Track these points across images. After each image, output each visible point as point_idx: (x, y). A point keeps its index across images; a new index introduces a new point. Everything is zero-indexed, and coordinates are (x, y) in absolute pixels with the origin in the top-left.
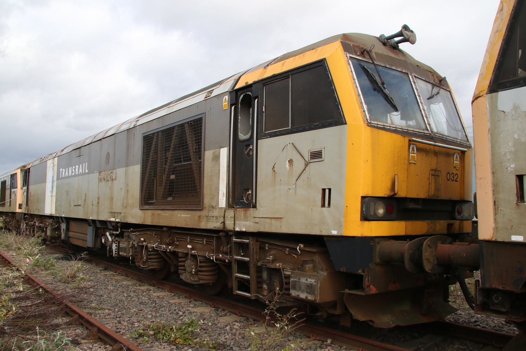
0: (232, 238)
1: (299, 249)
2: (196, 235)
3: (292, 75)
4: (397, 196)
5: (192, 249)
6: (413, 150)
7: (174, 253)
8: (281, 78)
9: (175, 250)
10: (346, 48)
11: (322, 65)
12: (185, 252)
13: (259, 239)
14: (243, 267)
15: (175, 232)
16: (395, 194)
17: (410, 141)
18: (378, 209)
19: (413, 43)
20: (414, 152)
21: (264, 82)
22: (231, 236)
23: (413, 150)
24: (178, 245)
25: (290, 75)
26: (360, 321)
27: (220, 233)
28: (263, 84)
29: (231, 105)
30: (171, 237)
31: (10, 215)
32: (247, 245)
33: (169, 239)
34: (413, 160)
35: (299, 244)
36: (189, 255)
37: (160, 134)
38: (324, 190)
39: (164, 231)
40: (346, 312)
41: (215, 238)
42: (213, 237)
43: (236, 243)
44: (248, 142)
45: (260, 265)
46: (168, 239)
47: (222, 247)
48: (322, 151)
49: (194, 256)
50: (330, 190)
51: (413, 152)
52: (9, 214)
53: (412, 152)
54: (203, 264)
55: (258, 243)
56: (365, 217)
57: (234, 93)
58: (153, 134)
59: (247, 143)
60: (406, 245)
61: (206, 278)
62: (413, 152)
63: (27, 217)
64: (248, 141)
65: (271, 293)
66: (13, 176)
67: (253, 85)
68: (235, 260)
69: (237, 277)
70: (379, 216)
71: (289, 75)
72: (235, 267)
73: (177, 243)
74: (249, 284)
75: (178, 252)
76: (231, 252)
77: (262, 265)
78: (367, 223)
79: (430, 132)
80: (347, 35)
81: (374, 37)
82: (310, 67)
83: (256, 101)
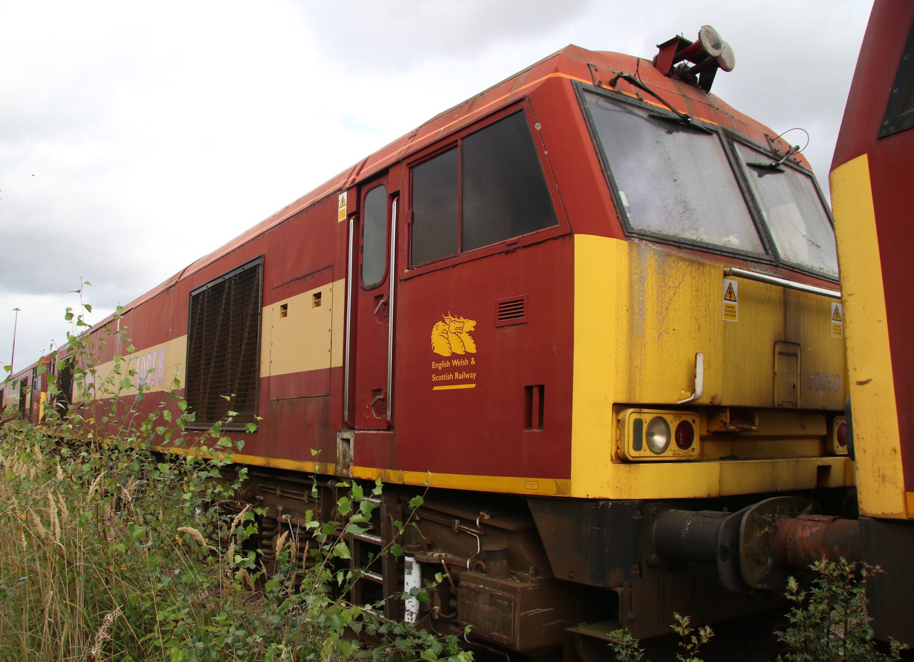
6: (730, 293)
15: (258, 477)
20: (732, 296)
24: (262, 501)
25: (460, 142)
28: (408, 165)
30: (250, 485)
33: (246, 489)
34: (731, 315)
35: (481, 510)
46: (244, 490)
51: (731, 297)
58: (221, 285)
60: (718, 521)
62: (731, 297)
67: (391, 171)
68: (355, 539)
71: (457, 141)
73: (262, 498)
81: (644, 59)
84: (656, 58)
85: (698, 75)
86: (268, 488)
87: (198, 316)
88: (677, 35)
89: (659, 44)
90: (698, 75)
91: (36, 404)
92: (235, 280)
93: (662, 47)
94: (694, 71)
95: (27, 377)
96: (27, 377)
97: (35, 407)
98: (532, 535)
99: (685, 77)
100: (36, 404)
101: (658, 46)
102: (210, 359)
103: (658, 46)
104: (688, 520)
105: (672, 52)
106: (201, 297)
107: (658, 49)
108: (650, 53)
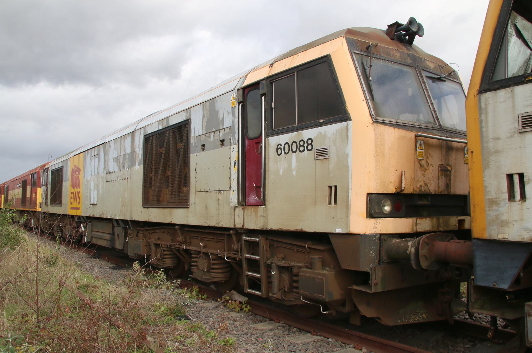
0: (242, 236)
1: (307, 247)
2: (208, 233)
3: (297, 71)
4: (403, 192)
5: (204, 247)
7: (187, 251)
8: (287, 75)
9: (188, 248)
10: (351, 44)
11: (326, 61)
12: (199, 250)
13: (268, 237)
14: (254, 265)
16: (402, 191)
17: (416, 136)
18: (384, 206)
19: (421, 36)
21: (270, 79)
22: (242, 234)
23: (421, 146)
26: (367, 318)
27: (230, 230)
28: (270, 81)
29: (239, 103)
31: (31, 214)
32: (256, 244)
36: (201, 253)
37: (171, 131)
38: (330, 187)
39: (176, 229)
40: (356, 310)
41: (226, 236)
42: (224, 234)
43: (246, 241)
44: (257, 140)
45: (270, 263)
47: (233, 245)
48: (327, 148)
49: (207, 254)
50: (336, 187)
51: (421, 148)
52: (29, 213)
53: (420, 148)
54: (214, 262)
55: (268, 242)
56: (371, 215)
57: (241, 91)
59: (256, 141)
61: (218, 276)
63: (46, 216)
64: (257, 138)
65: (281, 292)
66: (33, 175)
69: (247, 276)
70: (385, 212)
71: (295, 72)
72: (245, 265)
74: (260, 282)
75: (191, 250)
76: (241, 250)
77: (272, 263)
78: (372, 220)
79: (439, 127)
80: (353, 29)
82: (321, 61)
83: (263, 97)
84: (387, 30)
85: (407, 37)
86: (194, 236)
87: (149, 148)
88: (397, 21)
89: (388, 25)
90: (407, 37)
91: (34, 194)
92: (173, 131)
93: (389, 26)
94: (405, 35)
95: (27, 179)
96: (27, 179)
97: (34, 196)
98: (332, 251)
99: (400, 40)
100: (34, 194)
101: (388, 26)
102: (158, 170)
103: (388, 26)
104: (396, 241)
105: (394, 29)
106: (151, 138)
107: (388, 27)
108: (385, 28)
